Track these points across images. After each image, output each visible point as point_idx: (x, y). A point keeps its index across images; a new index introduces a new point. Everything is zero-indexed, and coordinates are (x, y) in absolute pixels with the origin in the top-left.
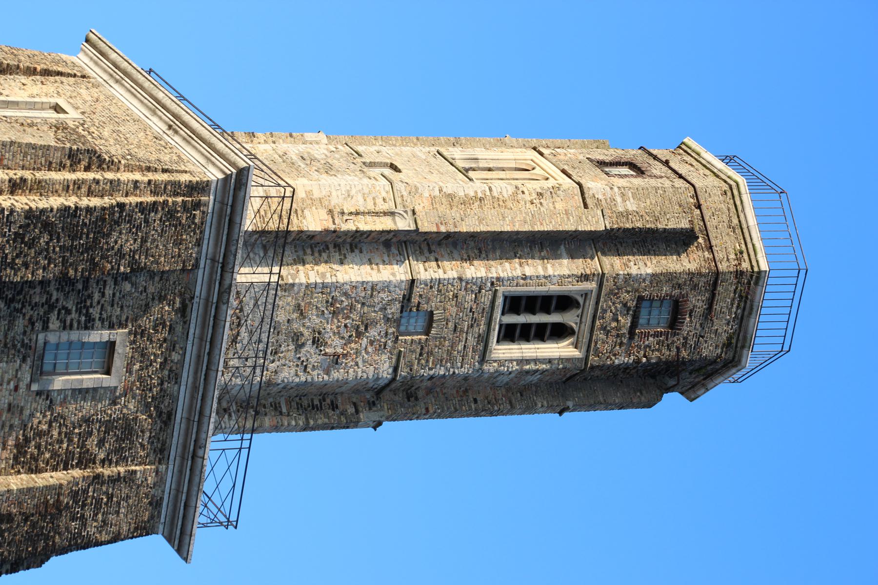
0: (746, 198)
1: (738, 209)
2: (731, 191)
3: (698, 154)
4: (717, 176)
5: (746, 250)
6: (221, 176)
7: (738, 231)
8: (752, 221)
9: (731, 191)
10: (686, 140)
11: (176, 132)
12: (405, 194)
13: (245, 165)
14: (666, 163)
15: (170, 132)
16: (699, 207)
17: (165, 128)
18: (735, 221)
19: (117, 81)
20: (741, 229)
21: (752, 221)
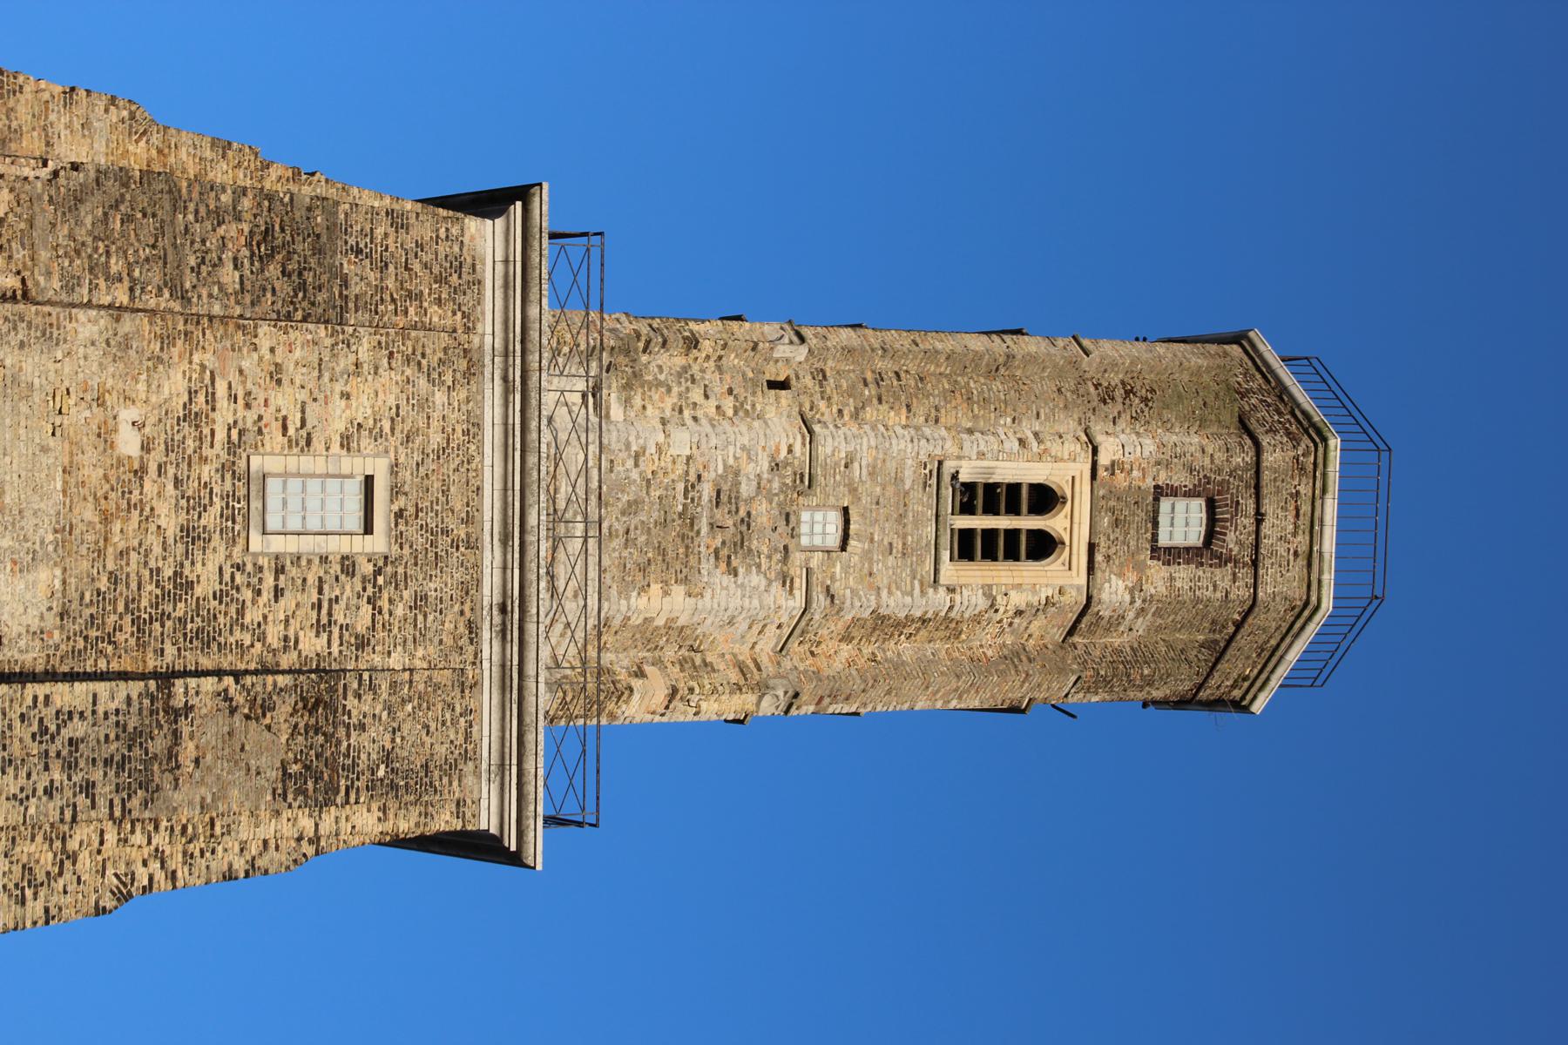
0: (1312, 629)
1: (1291, 632)
2: (1304, 610)
3: (1324, 490)
4: (1309, 565)
5: (1257, 683)
6: (494, 830)
7: (1266, 654)
8: (1293, 656)
9: (1304, 610)
10: (1335, 443)
11: (503, 632)
12: (817, 617)
13: (530, 862)
14: (1259, 518)
15: (497, 619)
16: (1239, 626)
17: (497, 599)
18: (1273, 642)
19: (505, 379)
20: (1271, 656)
21: (1293, 656)
